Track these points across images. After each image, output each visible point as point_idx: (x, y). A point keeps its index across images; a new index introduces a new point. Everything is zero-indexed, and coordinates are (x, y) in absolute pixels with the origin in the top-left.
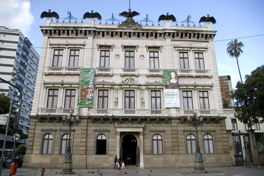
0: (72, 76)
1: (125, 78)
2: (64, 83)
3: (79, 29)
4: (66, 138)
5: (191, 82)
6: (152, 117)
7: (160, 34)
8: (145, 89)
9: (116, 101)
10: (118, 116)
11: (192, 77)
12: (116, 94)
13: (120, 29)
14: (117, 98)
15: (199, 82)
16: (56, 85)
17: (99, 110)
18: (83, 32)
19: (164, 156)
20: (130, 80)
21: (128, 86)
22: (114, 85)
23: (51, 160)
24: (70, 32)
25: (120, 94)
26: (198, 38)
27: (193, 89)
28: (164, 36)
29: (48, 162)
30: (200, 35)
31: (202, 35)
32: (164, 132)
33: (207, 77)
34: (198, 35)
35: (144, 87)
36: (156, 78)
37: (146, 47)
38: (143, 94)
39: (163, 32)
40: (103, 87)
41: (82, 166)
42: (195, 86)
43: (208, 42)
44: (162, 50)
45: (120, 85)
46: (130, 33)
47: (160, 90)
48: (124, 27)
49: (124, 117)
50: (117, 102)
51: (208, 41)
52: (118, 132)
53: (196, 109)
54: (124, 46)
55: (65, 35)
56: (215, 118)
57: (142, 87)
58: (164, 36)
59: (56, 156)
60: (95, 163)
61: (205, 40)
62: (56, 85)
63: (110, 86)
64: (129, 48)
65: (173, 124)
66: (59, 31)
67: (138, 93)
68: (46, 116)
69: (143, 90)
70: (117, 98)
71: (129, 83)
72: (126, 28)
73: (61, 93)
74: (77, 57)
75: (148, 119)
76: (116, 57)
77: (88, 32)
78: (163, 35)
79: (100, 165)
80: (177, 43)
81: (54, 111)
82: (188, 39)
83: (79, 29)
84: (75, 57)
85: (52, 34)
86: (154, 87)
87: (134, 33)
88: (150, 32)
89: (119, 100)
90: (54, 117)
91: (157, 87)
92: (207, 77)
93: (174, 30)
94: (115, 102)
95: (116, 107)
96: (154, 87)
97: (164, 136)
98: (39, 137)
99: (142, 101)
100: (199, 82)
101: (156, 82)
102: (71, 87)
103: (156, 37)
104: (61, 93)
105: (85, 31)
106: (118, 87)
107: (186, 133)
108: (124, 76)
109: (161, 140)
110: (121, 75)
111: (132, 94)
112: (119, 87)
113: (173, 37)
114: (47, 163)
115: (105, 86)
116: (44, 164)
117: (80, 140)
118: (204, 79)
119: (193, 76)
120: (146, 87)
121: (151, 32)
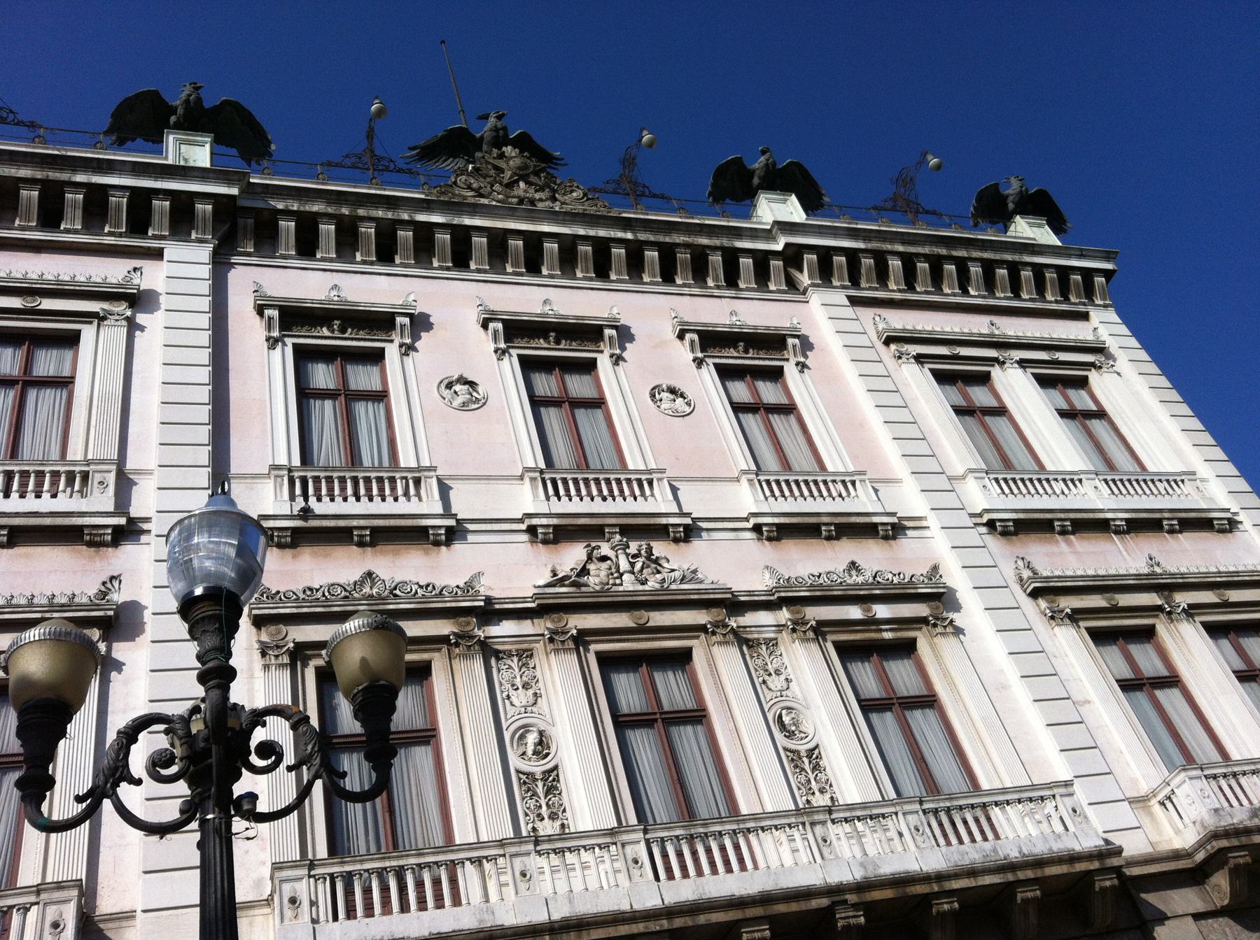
1: (572, 556)
6: (972, 872)
7: (762, 261)
8: (785, 636)
9: (538, 768)
12: (521, 697)
14: (532, 738)
17: (348, 878)
18: (120, 202)
20: (624, 564)
21: (621, 620)
25: (562, 698)
28: (792, 284)
35: (764, 618)
37: (681, 336)
38: (776, 683)
39: (779, 247)
42: (1168, 587)
46: (534, 242)
47: (911, 634)
50: (552, 779)
57: (750, 619)
61: (1064, 307)
64: (546, 338)
67: (721, 673)
69: (768, 642)
70: (541, 733)
71: (628, 583)
74: (48, 393)
76: (446, 393)
78: (776, 264)
83: (80, 178)
84: (32, 394)
86: (855, 612)
87: (568, 249)
88: (686, 245)
91: (882, 611)
96: (855, 612)
99: (791, 744)
101: (853, 565)
103: (731, 280)
106: (526, 627)
108: (564, 533)
110: (532, 530)
111: (671, 689)
113: (855, 282)
118: (1188, 541)
119: (1107, 521)
120: (784, 615)
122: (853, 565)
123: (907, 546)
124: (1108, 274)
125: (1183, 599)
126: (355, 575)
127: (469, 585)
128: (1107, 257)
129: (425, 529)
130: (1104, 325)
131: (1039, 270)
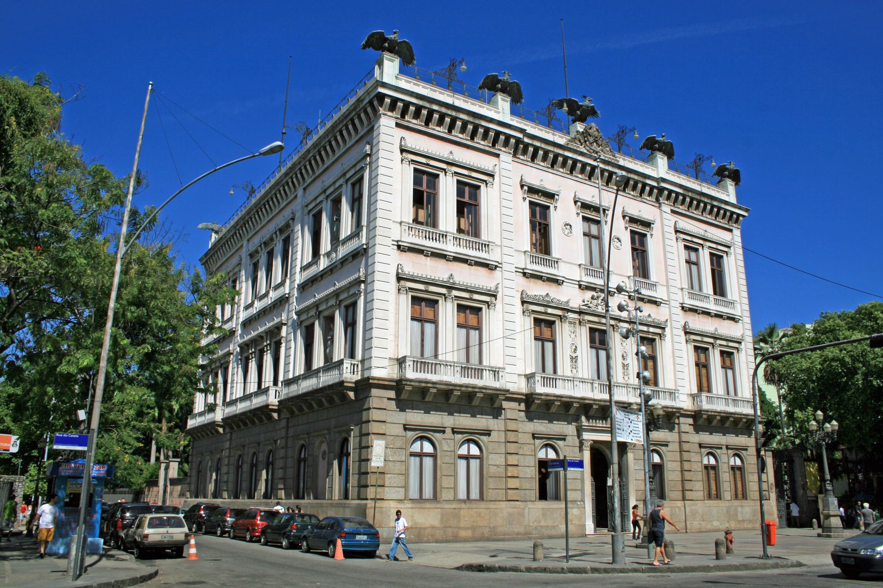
0: (470, 265)
2: (454, 284)
3: (484, 123)
4: (466, 453)
5: (438, 271)
9: (574, 355)
10: (591, 400)
11: (707, 313)
12: (573, 336)
13: (570, 150)
15: (464, 275)
16: (432, 289)
19: (483, 505)
22: (568, 311)
23: (442, 518)
24: (459, 124)
26: (427, 124)
27: (444, 295)
29: (433, 523)
30: (481, 130)
31: (487, 130)
32: (488, 433)
33: (732, 319)
34: (476, 127)
36: (474, 267)
40: (546, 313)
41: (518, 534)
43: (498, 156)
44: (558, 204)
45: (580, 313)
48: (582, 149)
49: (602, 403)
51: (498, 152)
52: (586, 440)
53: (446, 361)
54: (529, 187)
55: (440, 129)
56: (452, 390)
58: (657, 200)
59: (454, 506)
60: (543, 523)
62: (432, 289)
63: (559, 312)
65: (509, 414)
66: (431, 112)
68: (430, 385)
72: (585, 151)
73: (447, 312)
75: (479, 395)
77: (502, 137)
78: (655, 191)
79: (554, 527)
80: (685, 224)
81: (434, 367)
82: (441, 131)
83: (484, 123)
85: (476, 135)
89: (578, 353)
90: (549, 398)
91: (652, 330)
92: (732, 319)
93: (681, 186)
94: (572, 358)
95: (574, 371)
97: (440, 444)
98: (398, 445)
100: (464, 275)
101: (649, 315)
102: (471, 299)
104: (447, 312)
105: (498, 134)
107: (537, 441)
109: (480, 458)
112: (576, 316)
114: (433, 527)
115: (550, 311)
116: (425, 529)
117: (503, 460)
121: (636, 177)
122: (649, 315)
123: (663, 309)
124: (743, 216)
125: (719, 342)
126: (544, 294)
127: (567, 302)
128: (747, 210)
129: (557, 280)
130: (735, 237)
131: (726, 211)
